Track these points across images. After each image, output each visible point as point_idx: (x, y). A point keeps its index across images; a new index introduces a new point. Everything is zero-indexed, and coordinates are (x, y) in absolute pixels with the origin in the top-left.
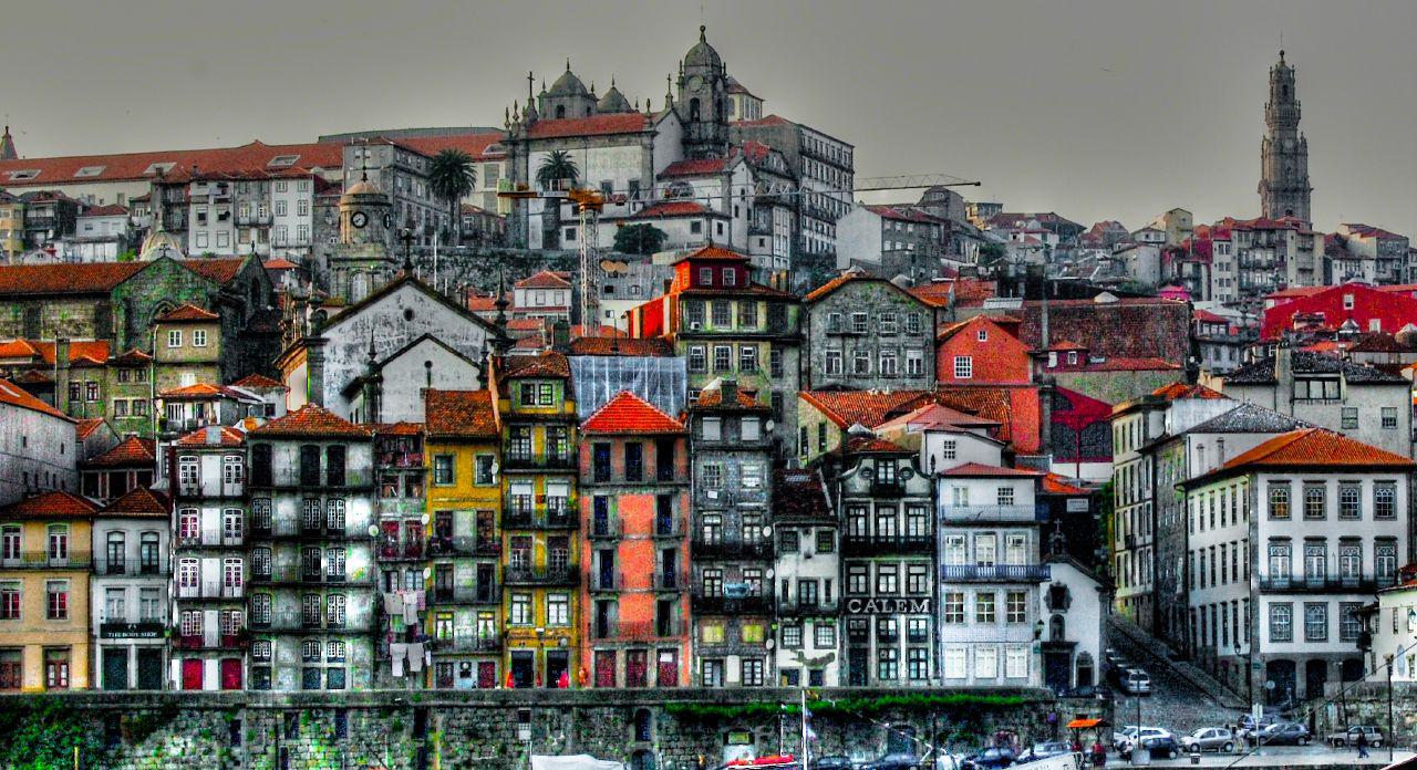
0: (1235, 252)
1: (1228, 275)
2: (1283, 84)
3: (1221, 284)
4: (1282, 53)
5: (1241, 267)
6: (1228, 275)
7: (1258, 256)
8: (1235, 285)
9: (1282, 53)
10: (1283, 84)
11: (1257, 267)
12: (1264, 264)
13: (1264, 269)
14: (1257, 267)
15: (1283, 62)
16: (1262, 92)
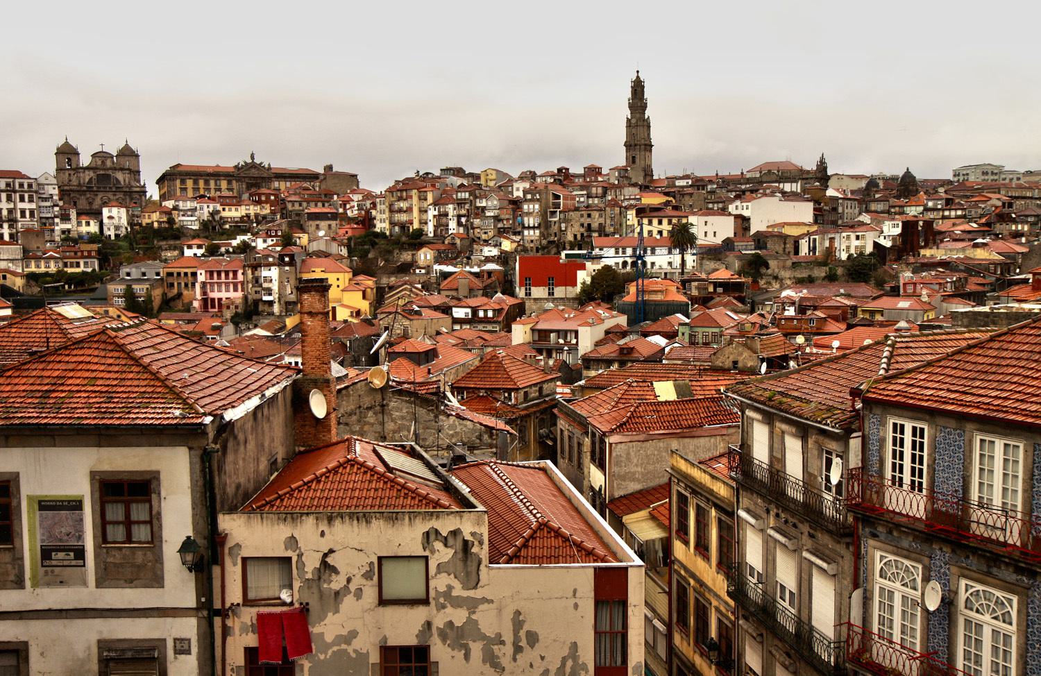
0: (387, 204)
1: (384, 216)
2: (638, 88)
3: (381, 222)
4: (638, 72)
5: (391, 211)
6: (384, 216)
7: (402, 205)
8: (387, 222)
9: (638, 72)
10: (638, 88)
11: (400, 211)
12: (405, 209)
13: (405, 212)
14: (400, 211)
15: (638, 77)
16: (628, 94)
